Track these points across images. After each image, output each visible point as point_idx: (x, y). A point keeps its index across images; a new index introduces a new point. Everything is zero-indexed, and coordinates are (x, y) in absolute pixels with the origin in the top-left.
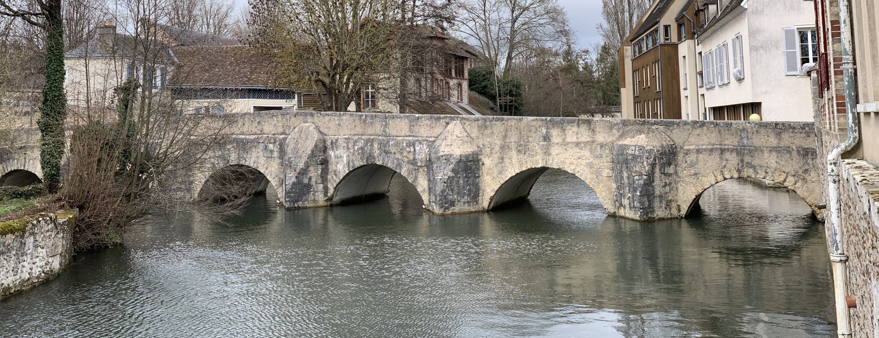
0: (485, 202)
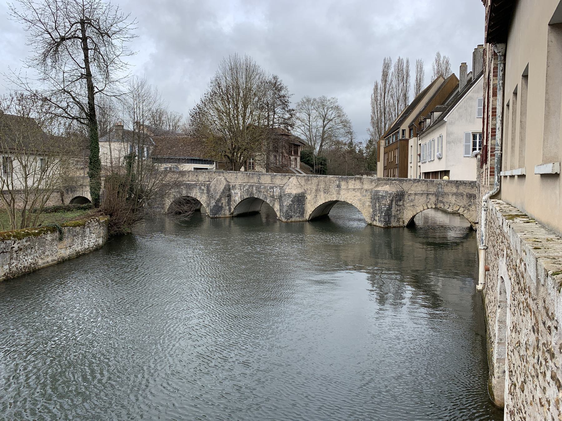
0: (307, 218)
